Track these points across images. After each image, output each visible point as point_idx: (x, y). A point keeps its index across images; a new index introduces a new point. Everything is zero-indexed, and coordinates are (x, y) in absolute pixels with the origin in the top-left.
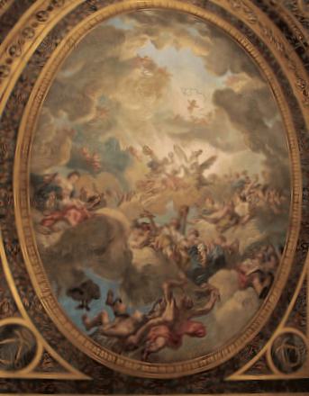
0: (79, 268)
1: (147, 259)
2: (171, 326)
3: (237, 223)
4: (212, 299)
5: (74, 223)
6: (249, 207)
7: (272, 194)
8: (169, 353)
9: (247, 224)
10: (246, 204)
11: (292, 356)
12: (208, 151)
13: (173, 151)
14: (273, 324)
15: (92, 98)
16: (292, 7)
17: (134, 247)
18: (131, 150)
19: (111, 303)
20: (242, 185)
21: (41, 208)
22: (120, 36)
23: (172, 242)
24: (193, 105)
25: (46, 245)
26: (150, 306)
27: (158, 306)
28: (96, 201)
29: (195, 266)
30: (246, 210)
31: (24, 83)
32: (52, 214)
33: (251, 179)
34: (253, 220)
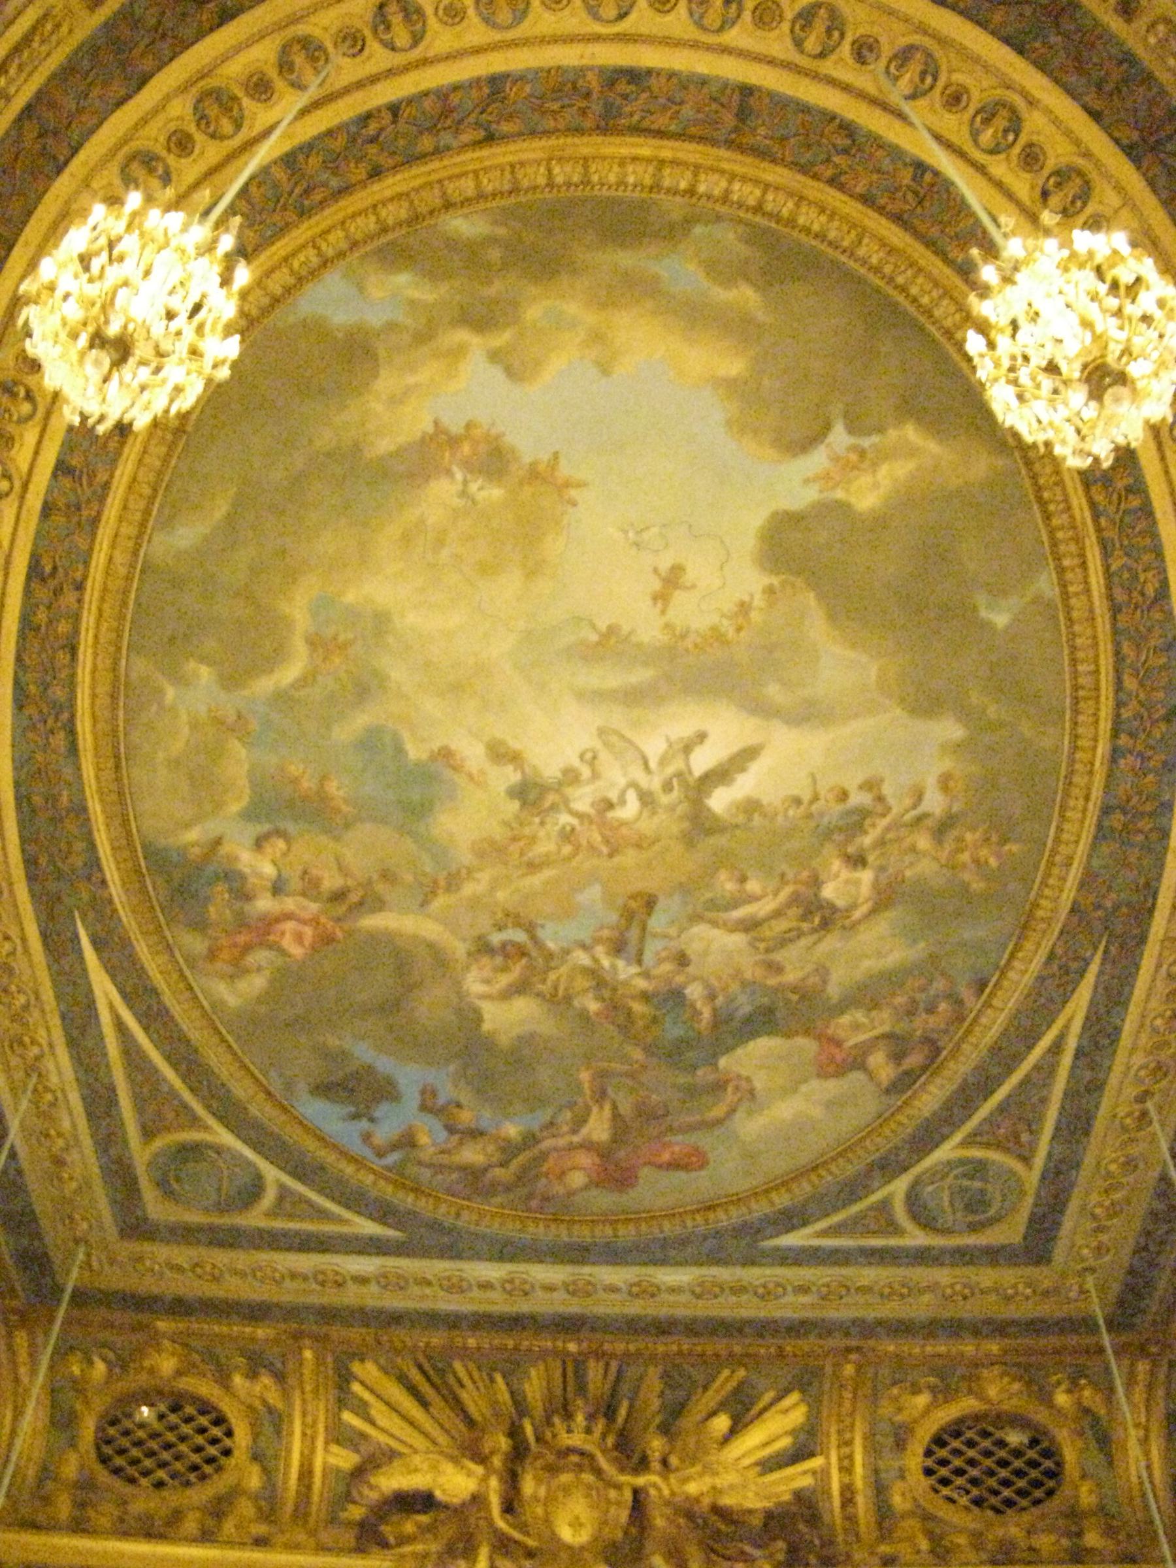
0: (333, 1042)
2: (604, 1153)
3: (825, 924)
4: (730, 1096)
5: (297, 951)
6: (876, 884)
7: (969, 837)
11: (975, 1204)
13: (597, 744)
14: (926, 1138)
15: (284, 607)
17: (483, 997)
18: (446, 754)
20: (857, 821)
21: (200, 925)
22: (356, 353)
24: (673, 581)
26: (544, 1116)
28: (354, 898)
29: (677, 1032)
30: (865, 890)
31: (52, 583)
33: (891, 801)
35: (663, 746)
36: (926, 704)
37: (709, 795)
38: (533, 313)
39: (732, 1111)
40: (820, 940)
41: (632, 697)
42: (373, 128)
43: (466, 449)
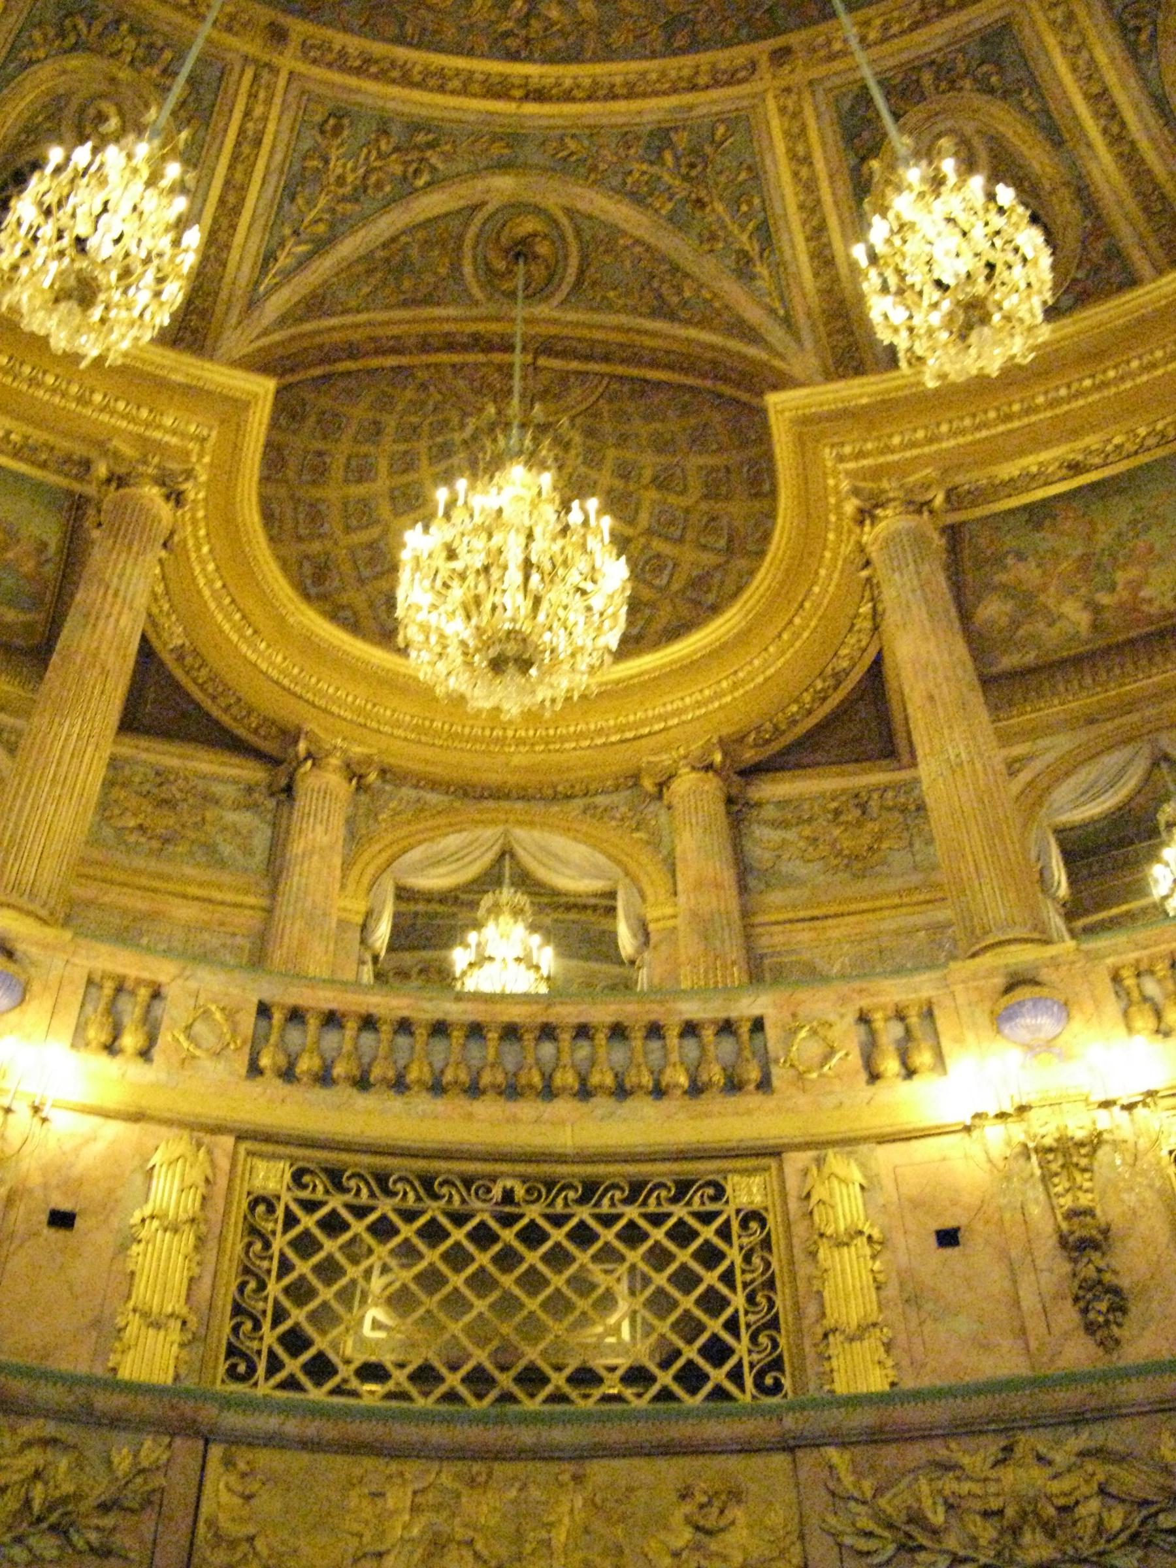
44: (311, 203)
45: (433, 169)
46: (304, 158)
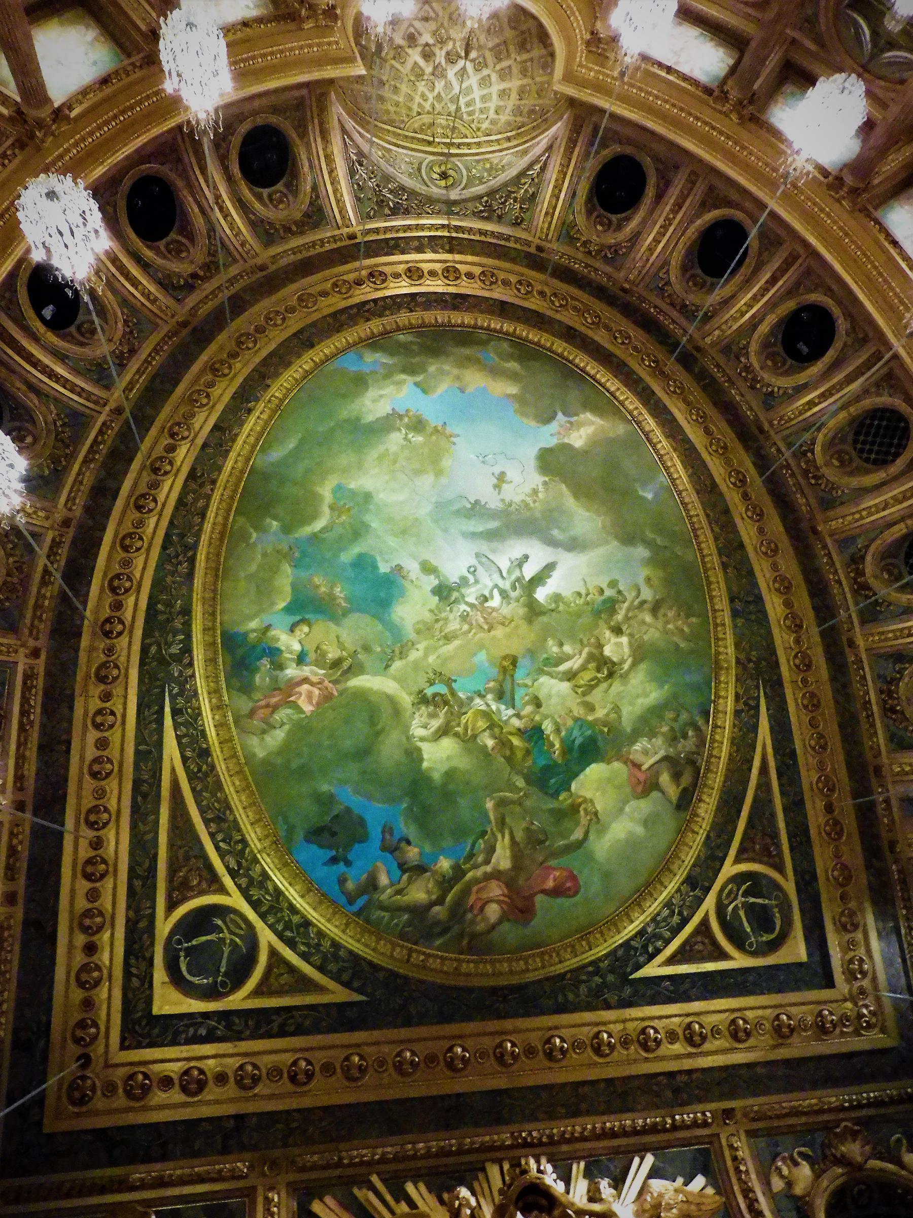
0: (325, 788)
1: (448, 758)
3: (611, 675)
4: (584, 820)
5: (308, 708)
8: (510, 933)
9: (632, 675)
10: (624, 640)
12: (538, 555)
13: (474, 562)
15: (320, 490)
16: (662, 289)
17: (422, 739)
18: (399, 568)
19: (393, 847)
20: (611, 606)
21: (247, 689)
22: (360, 382)
23: (493, 725)
24: (501, 478)
25: (261, 753)
27: (481, 844)
28: (345, 665)
29: (542, 762)
30: (626, 650)
32: (265, 697)
33: (625, 593)
34: (643, 666)
35: (509, 564)
36: (628, 539)
37: (534, 592)
38: (432, 369)
39: (587, 834)
40: (611, 685)
41: (492, 536)
42: (367, 307)
43: (406, 420)
44: (526, 191)
45: (481, 203)
46: (528, 209)
